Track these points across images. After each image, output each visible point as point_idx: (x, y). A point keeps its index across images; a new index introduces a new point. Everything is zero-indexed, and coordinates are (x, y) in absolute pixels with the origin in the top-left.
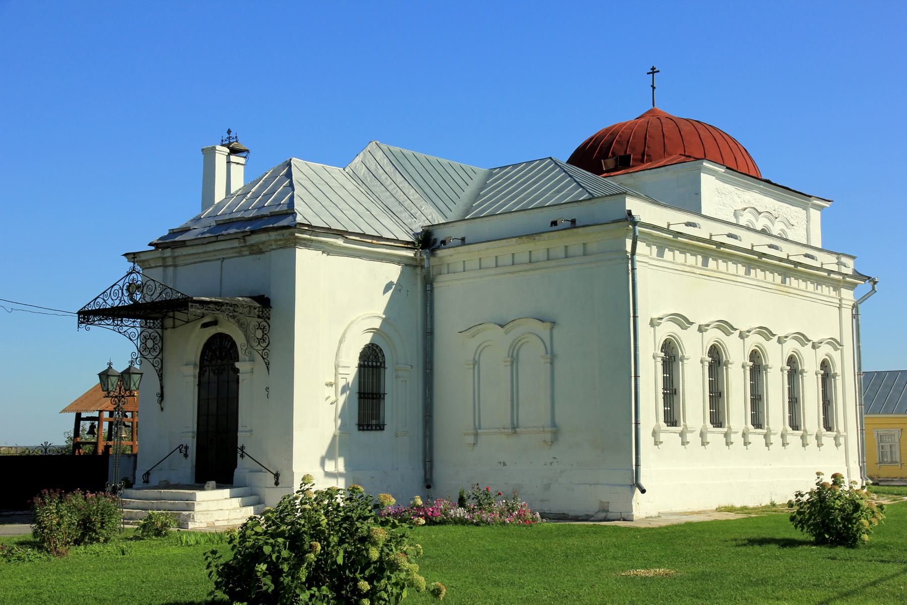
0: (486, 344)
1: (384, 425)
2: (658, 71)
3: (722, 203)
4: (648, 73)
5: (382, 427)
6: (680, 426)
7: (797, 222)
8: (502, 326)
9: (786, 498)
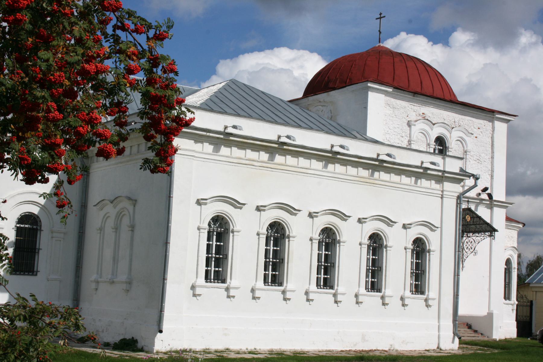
0: (108, 215)
1: (37, 271)
2: (384, 17)
3: (393, 115)
4: (377, 19)
5: (35, 273)
6: (226, 283)
7: (482, 132)
8: (112, 202)
9: (355, 345)
